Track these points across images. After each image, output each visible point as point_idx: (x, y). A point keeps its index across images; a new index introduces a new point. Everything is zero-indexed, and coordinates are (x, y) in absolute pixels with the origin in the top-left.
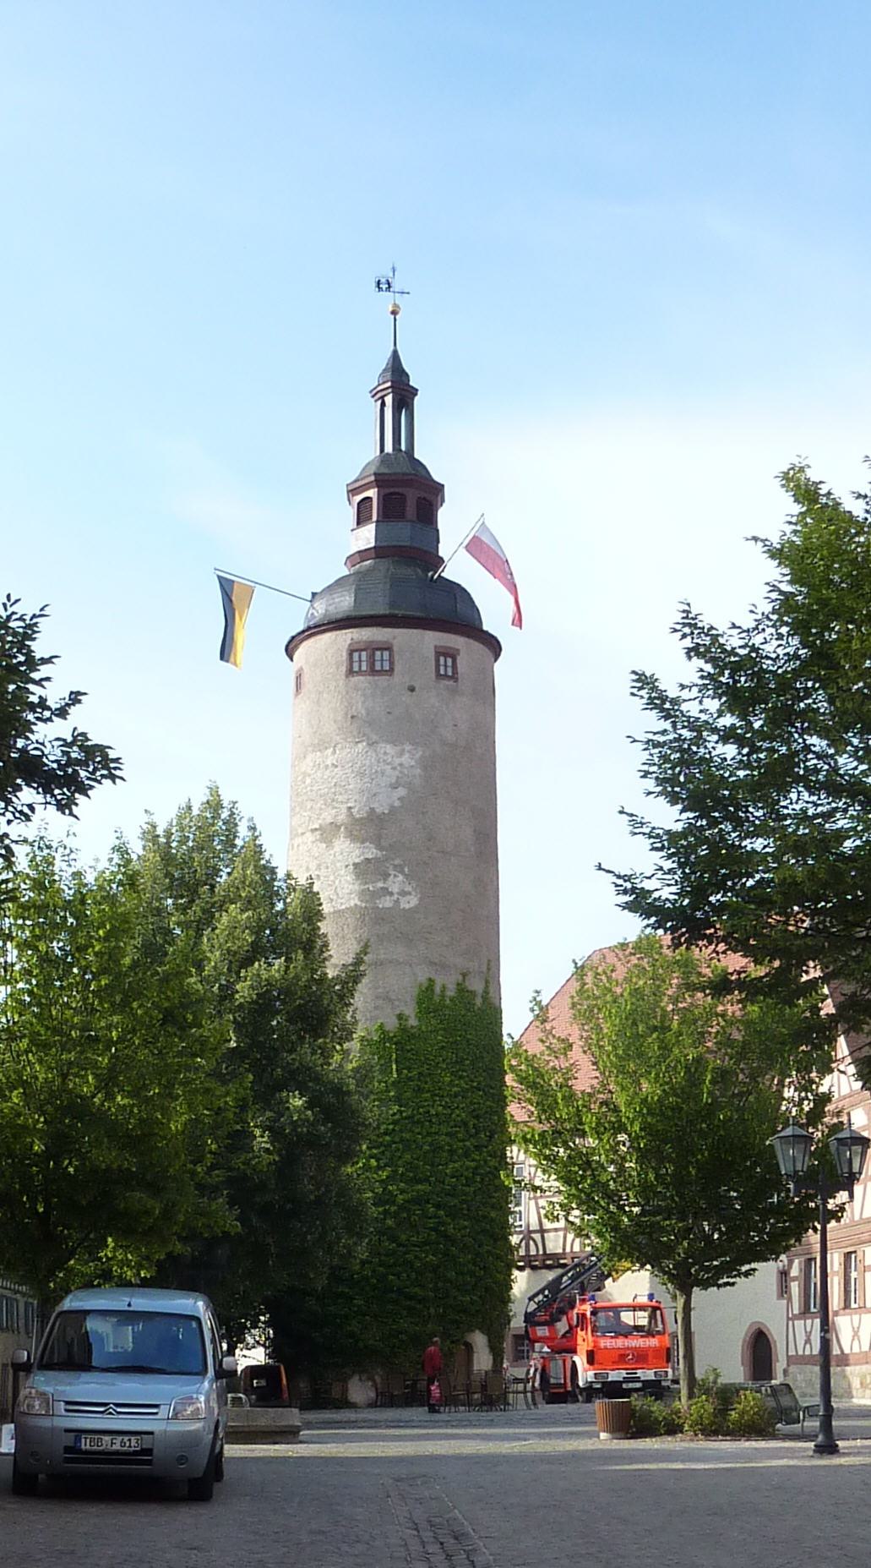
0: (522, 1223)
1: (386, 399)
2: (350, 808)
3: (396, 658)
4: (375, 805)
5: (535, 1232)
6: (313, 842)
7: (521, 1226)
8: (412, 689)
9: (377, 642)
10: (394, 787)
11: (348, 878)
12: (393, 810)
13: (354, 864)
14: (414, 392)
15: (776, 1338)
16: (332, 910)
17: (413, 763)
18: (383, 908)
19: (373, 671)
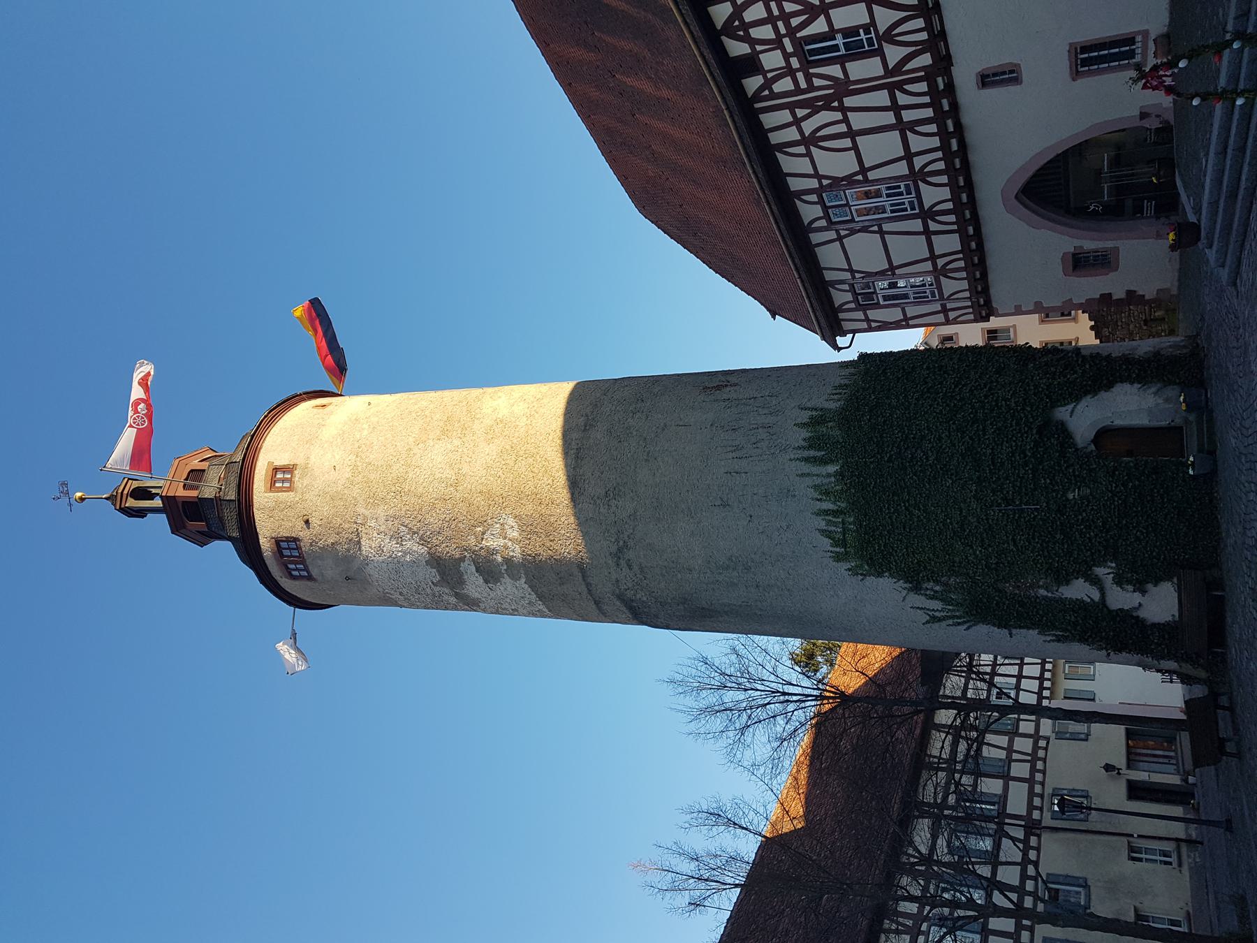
5: (935, 265)
8: (307, 522)
11: (502, 588)
13: (486, 581)
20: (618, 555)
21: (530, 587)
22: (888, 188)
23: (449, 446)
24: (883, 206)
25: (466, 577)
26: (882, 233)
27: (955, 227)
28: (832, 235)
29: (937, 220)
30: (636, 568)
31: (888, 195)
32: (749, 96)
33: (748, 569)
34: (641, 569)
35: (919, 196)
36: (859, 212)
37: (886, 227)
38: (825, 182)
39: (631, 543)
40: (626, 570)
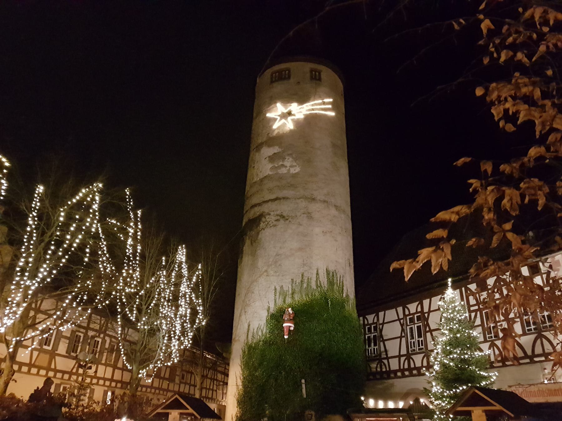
2: (268, 134)
5: (384, 359)
13: (269, 157)
16: (258, 179)
20: (282, 217)
22: (422, 341)
24: (414, 339)
26: (401, 337)
27: (402, 367)
28: (401, 316)
30: (275, 223)
31: (419, 341)
32: (468, 286)
36: (411, 329)
37: (404, 340)
38: (426, 315)
39: (287, 222)
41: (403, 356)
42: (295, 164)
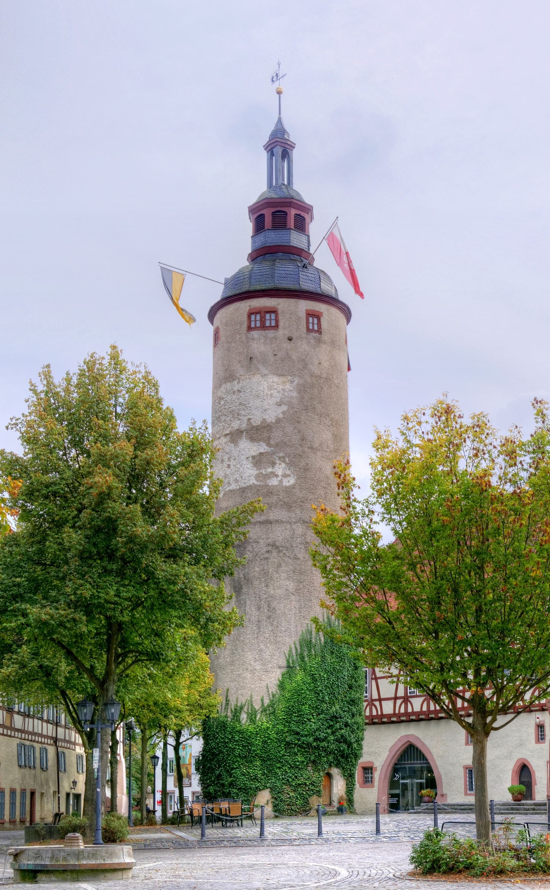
0: (367, 694)
1: (275, 150)
2: (249, 419)
3: (280, 317)
4: (266, 417)
6: (226, 443)
7: (366, 697)
8: (290, 339)
9: (266, 307)
10: (279, 404)
11: (249, 466)
12: (278, 421)
13: (253, 457)
14: (293, 147)
15: (534, 769)
16: (238, 487)
17: (291, 388)
18: (272, 486)
19: (263, 327)
20: (274, 545)
21: (251, 486)
23: (330, 442)
25: (256, 444)
27: (397, 712)
29: (407, 706)
30: (267, 555)
33: (269, 617)
34: (267, 558)
35: (417, 696)
39: (281, 554)
40: (265, 549)
41: (400, 698)
42: (288, 472)
